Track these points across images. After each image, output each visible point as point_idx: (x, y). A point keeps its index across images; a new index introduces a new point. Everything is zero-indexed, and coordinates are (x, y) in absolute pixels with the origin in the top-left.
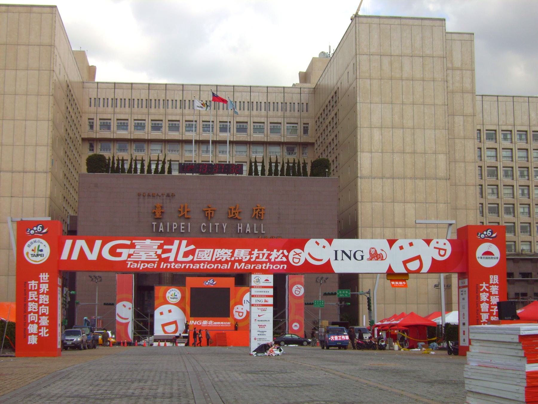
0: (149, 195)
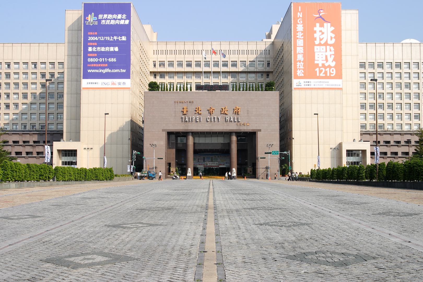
0: (180, 102)
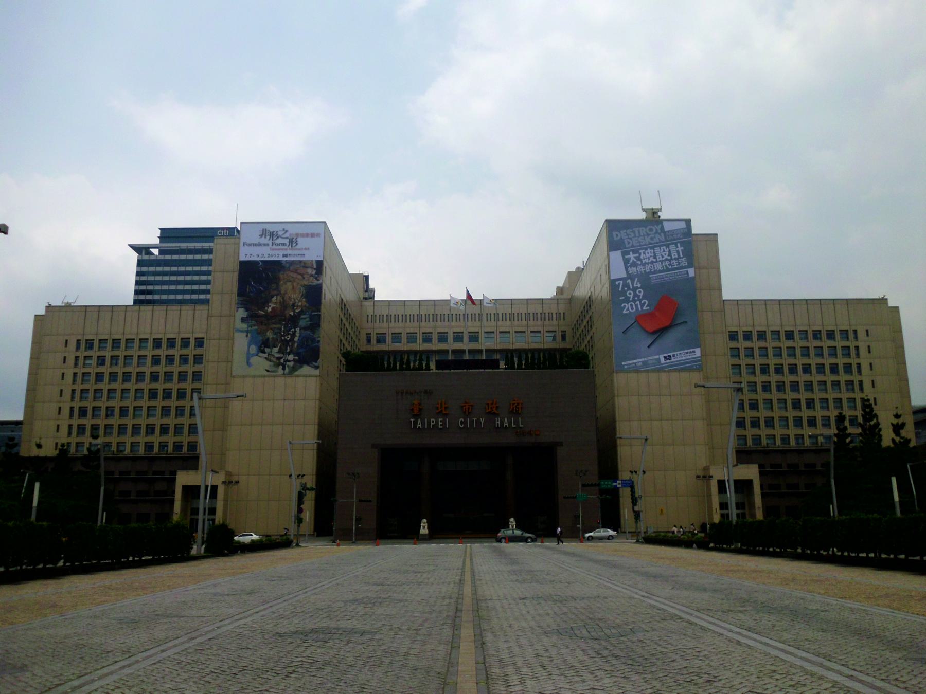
0: (407, 393)
